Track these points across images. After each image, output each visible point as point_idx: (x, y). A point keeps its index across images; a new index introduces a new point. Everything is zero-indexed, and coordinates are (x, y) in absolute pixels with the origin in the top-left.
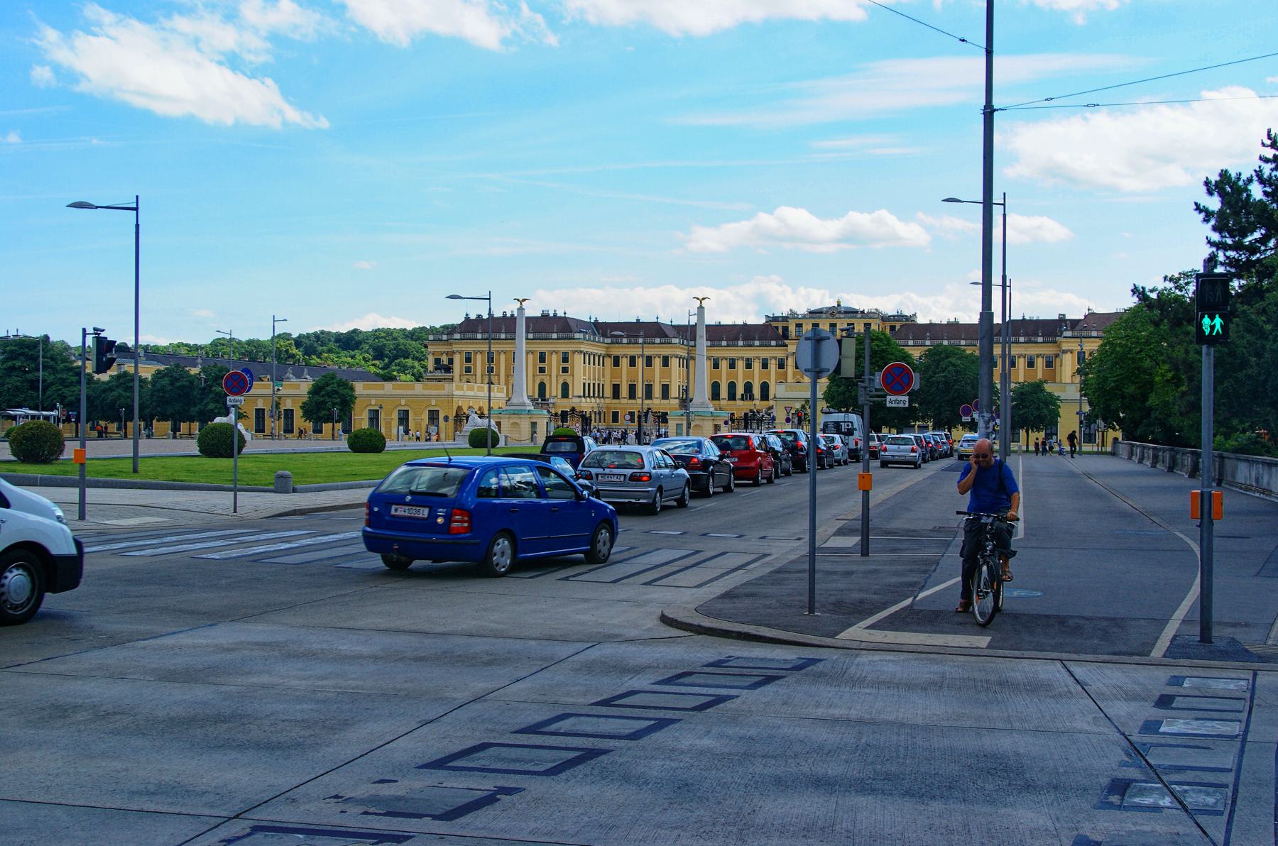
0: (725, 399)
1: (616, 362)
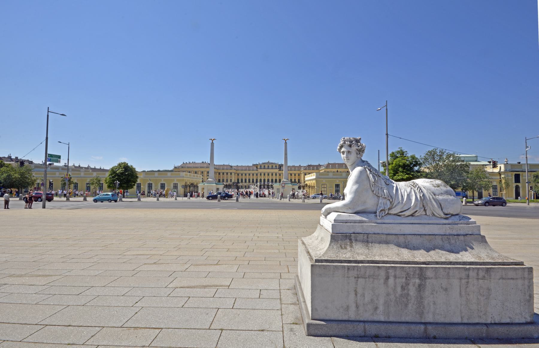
1: (219, 174)
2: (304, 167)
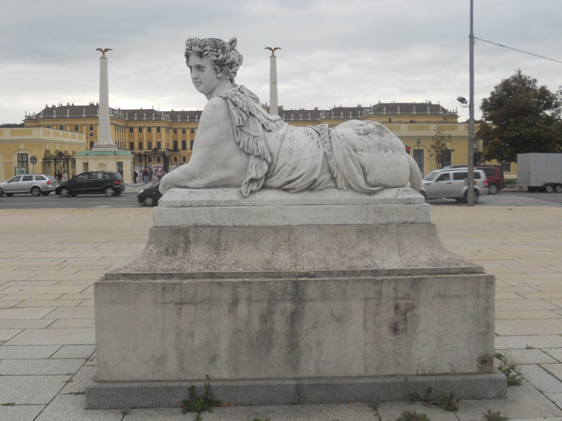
0: (189, 149)
2: (326, 112)
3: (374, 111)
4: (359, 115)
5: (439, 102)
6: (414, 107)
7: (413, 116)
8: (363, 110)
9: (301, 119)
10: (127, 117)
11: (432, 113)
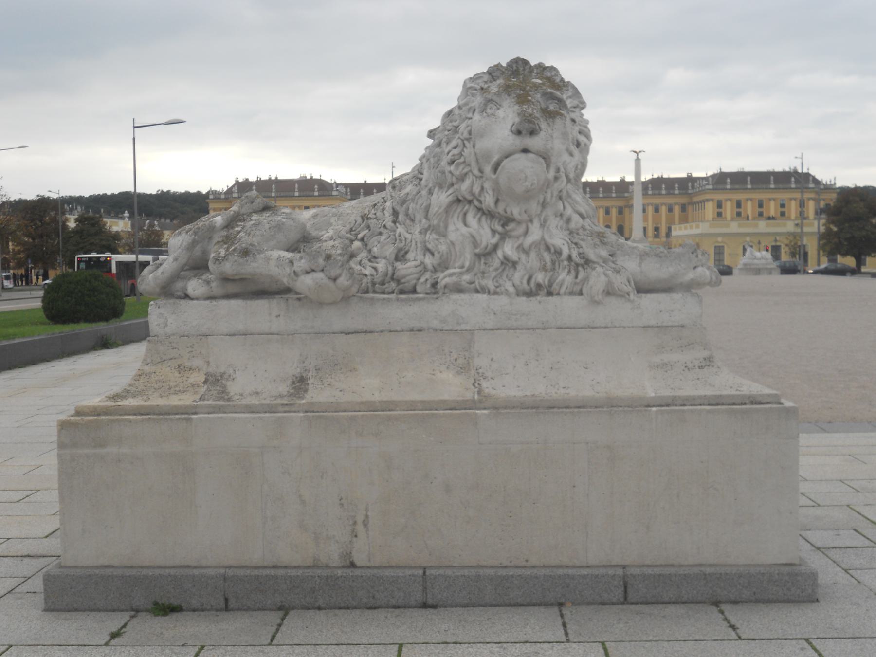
3: (713, 185)
4: (690, 188)
5: (808, 169)
6: (772, 178)
7: (771, 191)
8: (696, 182)
9: (601, 195)
10: (349, 194)
11: (799, 186)
